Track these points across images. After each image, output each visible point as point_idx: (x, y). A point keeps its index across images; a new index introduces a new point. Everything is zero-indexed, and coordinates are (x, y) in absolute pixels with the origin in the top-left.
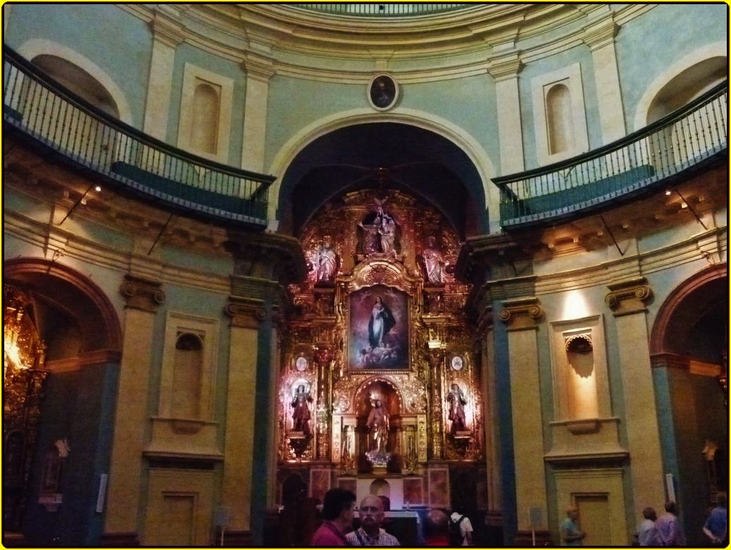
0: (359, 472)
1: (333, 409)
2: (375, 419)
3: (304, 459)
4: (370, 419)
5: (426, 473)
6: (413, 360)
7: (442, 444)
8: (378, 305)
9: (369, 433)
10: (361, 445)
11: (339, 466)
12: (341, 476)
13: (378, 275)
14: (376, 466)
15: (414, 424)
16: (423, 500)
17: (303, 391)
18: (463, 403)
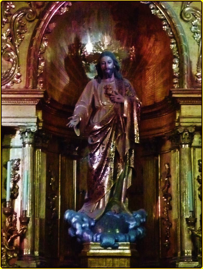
2: (94, 109)
9: (78, 158)
10: (51, 192)
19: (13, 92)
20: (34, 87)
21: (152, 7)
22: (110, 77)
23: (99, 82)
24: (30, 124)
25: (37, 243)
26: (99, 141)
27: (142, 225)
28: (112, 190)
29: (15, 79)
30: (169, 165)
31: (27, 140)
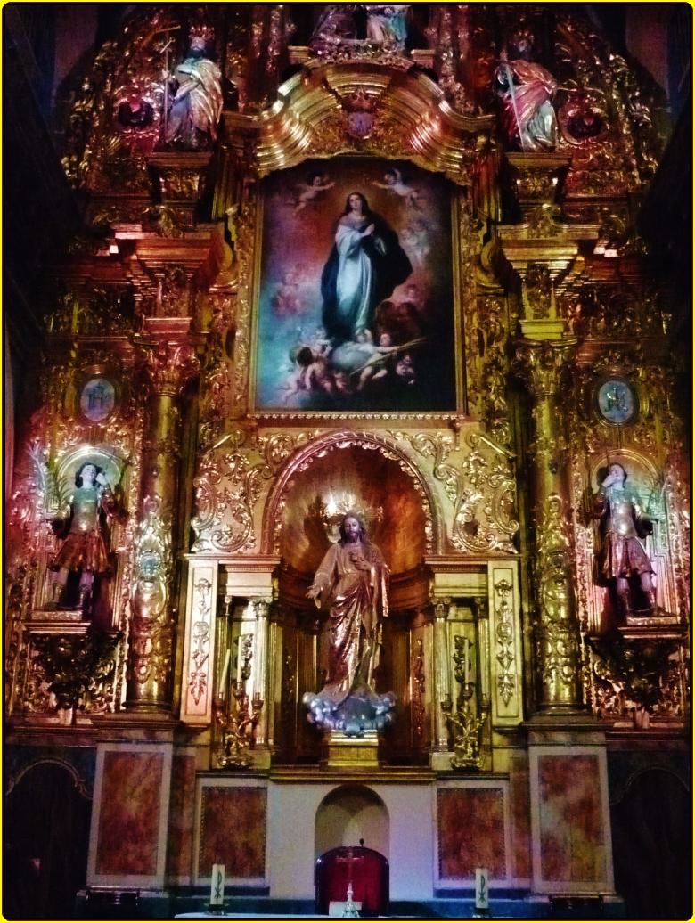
0: (275, 760)
1: (193, 539)
2: (337, 577)
3: (87, 714)
4: (322, 575)
5: (522, 765)
6: (469, 381)
7: (575, 660)
8: (356, 216)
9: (319, 633)
10: (287, 672)
11: (205, 738)
12: (213, 772)
13: (356, 121)
14: (338, 738)
15: (475, 593)
16: (509, 864)
17: (94, 483)
18: (643, 527)
19: (245, 558)
20: (270, 552)
21: (402, 463)
22: (354, 541)
23: (343, 547)
24: (263, 594)
25: (272, 730)
26: (342, 614)
27: (391, 710)
28: (357, 669)
29: (249, 543)
30: (421, 641)
31: (260, 613)
